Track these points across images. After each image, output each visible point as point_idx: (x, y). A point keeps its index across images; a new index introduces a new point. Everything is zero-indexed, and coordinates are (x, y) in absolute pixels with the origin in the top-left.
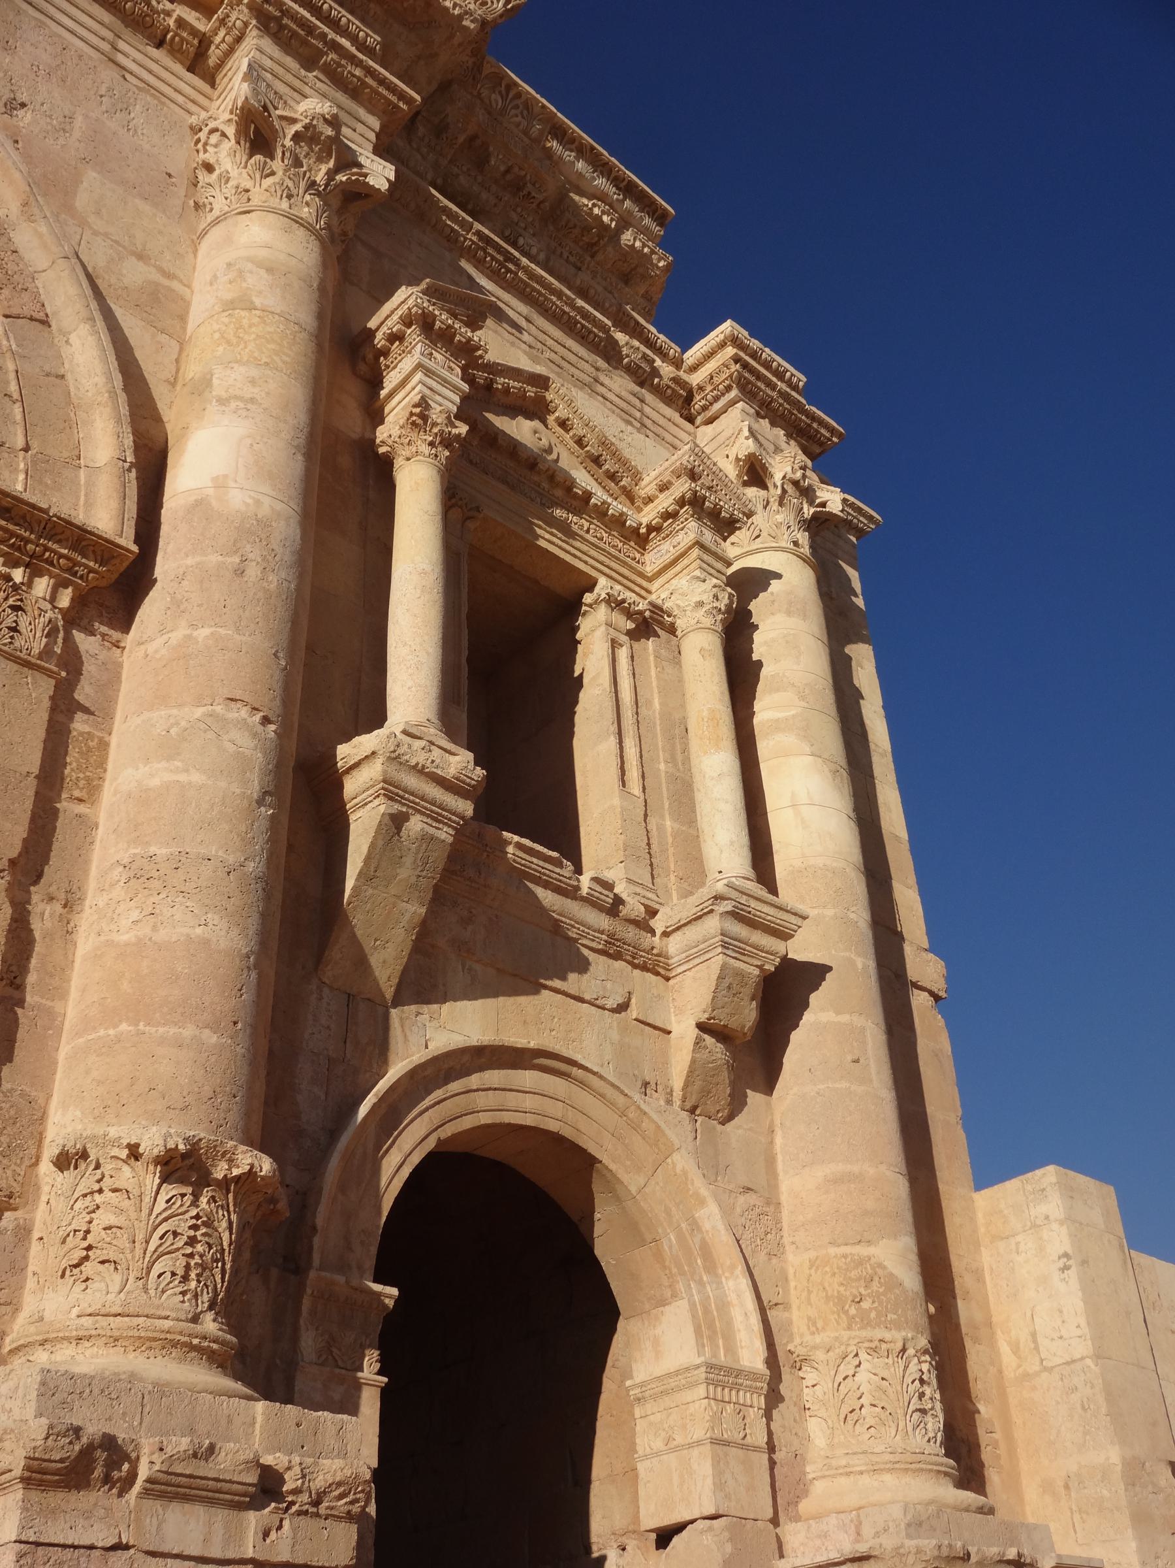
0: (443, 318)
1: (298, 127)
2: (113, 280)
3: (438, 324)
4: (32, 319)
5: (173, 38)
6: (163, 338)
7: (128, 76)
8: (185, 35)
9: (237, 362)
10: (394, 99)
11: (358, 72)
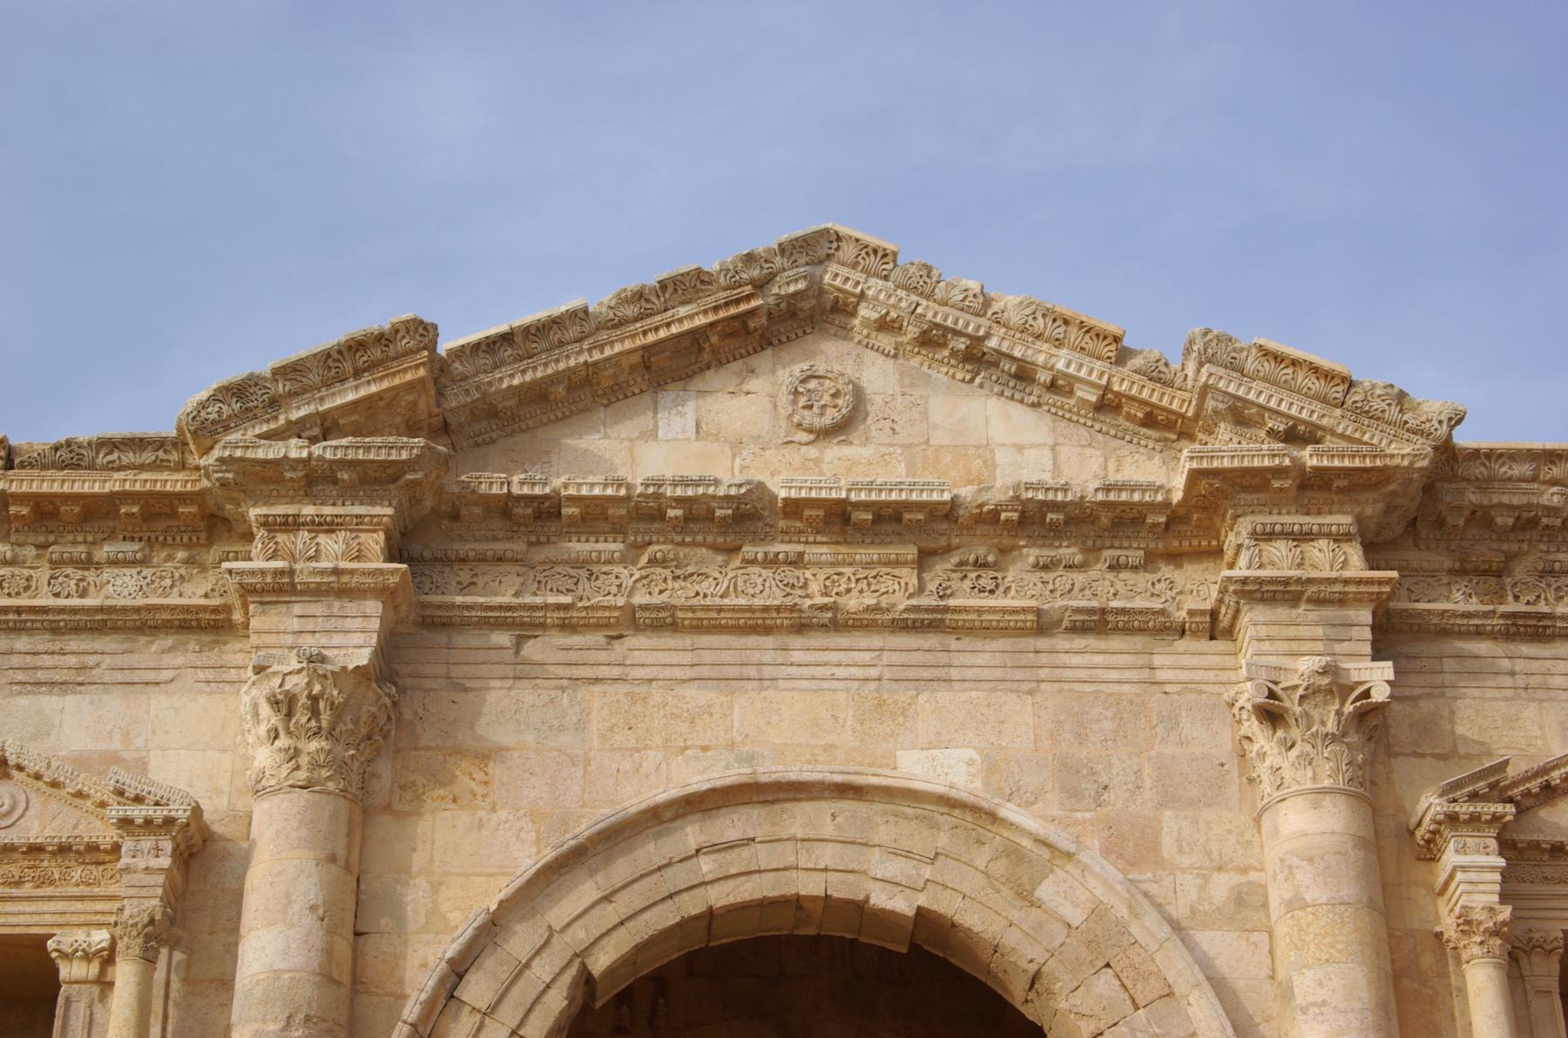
0: (1464, 809)
1: (1301, 691)
2: (1207, 907)
3: (1462, 817)
4: (1161, 997)
5: (1190, 626)
6: (1255, 937)
7: (1168, 688)
8: (1198, 619)
9: (1306, 966)
10: (1375, 589)
11: (1337, 588)
